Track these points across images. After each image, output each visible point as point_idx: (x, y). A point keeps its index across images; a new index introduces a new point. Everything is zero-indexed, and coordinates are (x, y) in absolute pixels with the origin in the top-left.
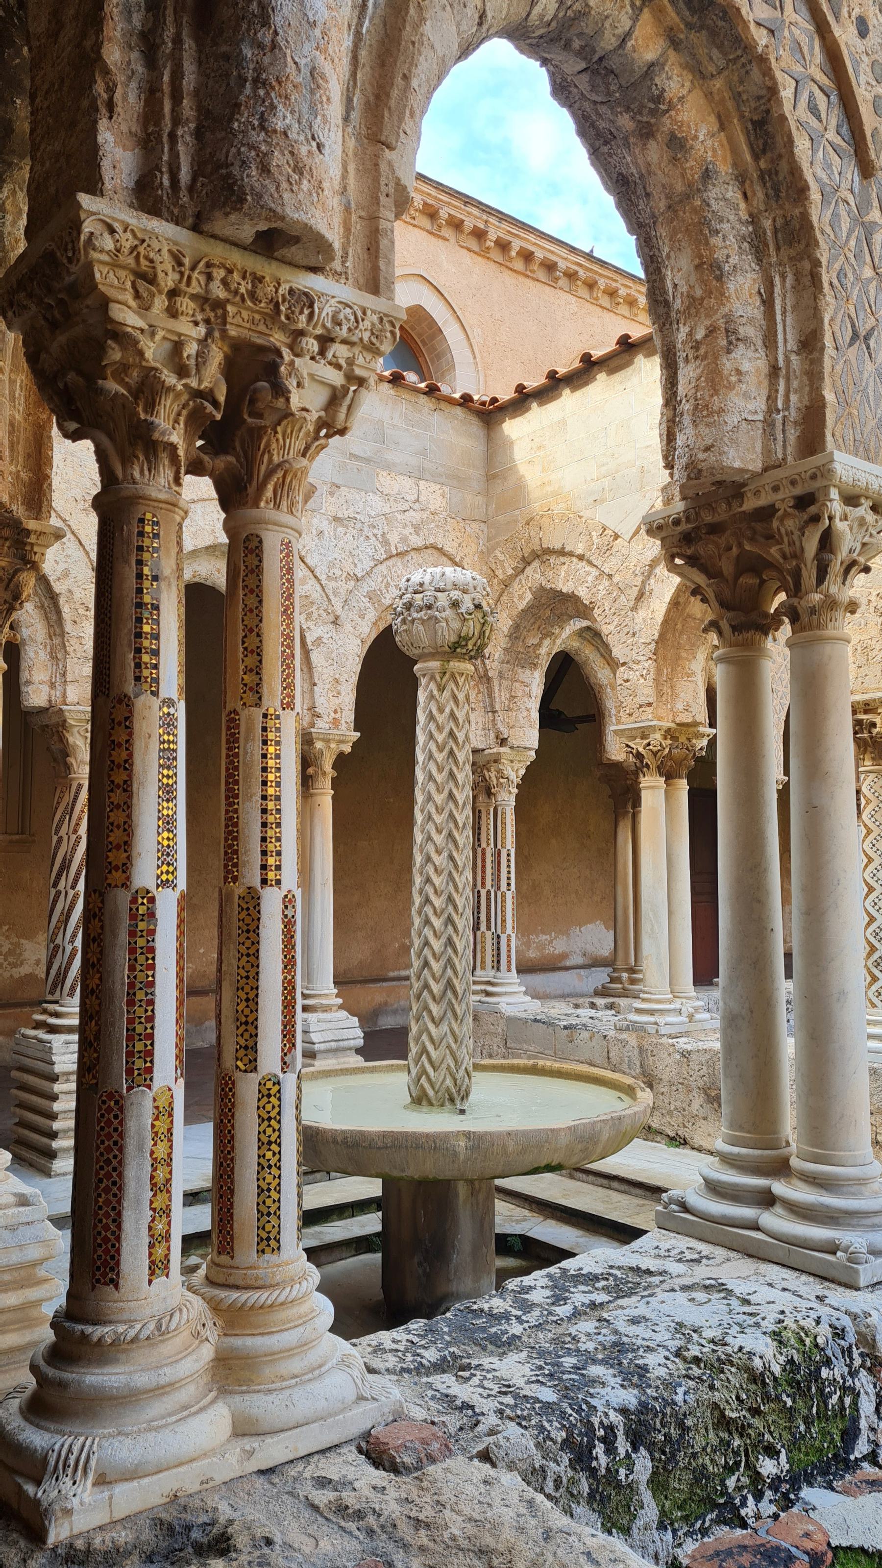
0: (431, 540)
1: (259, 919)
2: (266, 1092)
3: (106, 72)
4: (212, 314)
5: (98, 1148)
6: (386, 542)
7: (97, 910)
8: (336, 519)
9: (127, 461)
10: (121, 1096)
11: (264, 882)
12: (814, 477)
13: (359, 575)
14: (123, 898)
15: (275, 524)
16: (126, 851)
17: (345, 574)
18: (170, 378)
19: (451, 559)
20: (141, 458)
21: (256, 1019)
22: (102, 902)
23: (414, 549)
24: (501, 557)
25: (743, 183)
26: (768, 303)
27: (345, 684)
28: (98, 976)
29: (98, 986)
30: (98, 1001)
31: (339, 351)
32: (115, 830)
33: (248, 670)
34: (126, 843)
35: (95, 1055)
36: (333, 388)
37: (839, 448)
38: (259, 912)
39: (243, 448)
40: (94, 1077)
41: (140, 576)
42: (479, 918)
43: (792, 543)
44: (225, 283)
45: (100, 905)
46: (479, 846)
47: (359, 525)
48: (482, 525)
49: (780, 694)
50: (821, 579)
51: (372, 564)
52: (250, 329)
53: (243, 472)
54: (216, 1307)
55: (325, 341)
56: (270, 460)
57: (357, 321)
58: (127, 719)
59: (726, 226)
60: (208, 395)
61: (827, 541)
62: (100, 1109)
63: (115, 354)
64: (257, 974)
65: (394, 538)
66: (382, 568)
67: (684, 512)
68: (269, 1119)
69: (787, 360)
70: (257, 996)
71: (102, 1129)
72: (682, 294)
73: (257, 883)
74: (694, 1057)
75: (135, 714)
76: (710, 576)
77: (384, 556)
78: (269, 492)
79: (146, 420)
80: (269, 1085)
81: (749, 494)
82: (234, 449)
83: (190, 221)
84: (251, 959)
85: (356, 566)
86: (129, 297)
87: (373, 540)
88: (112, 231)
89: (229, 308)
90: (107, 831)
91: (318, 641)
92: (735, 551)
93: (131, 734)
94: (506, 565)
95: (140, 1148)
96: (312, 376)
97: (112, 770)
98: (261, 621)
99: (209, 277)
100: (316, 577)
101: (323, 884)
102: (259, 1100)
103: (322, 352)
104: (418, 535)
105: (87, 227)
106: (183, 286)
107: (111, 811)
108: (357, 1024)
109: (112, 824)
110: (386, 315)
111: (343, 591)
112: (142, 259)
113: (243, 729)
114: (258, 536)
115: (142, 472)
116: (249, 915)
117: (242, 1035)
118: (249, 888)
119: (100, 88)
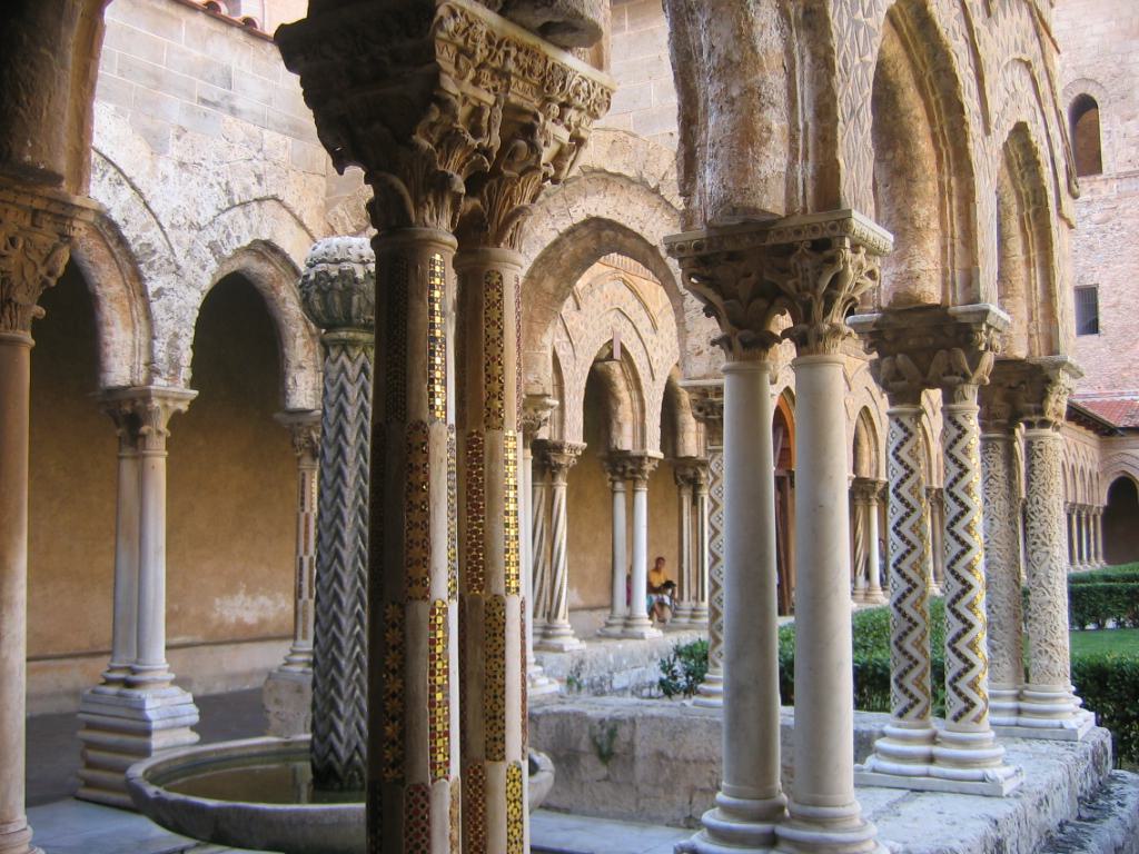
0: (273, 192)
1: (504, 624)
2: (512, 778)
4: (499, 84)
5: (407, 834)
6: (228, 192)
7: (397, 621)
8: (182, 164)
9: (419, 205)
10: (427, 788)
12: (833, 228)
13: (202, 225)
15: (513, 263)
16: (425, 567)
17: (188, 223)
19: (291, 212)
20: (432, 204)
21: (504, 714)
22: (403, 613)
23: (256, 200)
24: (342, 214)
26: (791, 76)
27: (184, 339)
28: (400, 681)
29: (400, 690)
30: (401, 704)
31: (572, 114)
32: (414, 546)
34: (425, 559)
35: (400, 752)
36: (562, 146)
37: (855, 209)
38: (504, 617)
39: (488, 192)
40: (399, 772)
42: (300, 586)
43: (805, 279)
44: (516, 59)
45: (401, 616)
46: (303, 510)
47: (203, 171)
48: (321, 178)
49: (582, 362)
50: (827, 312)
51: (216, 213)
52: (522, 97)
53: (486, 214)
55: (564, 106)
56: (511, 205)
57: (589, 93)
58: (424, 444)
60: (487, 152)
61: (837, 282)
62: (407, 800)
64: (504, 673)
65: (237, 188)
66: (224, 218)
67: (707, 239)
68: (515, 801)
70: (504, 693)
71: (411, 817)
72: (719, 56)
74: (542, 721)
75: (431, 440)
76: (724, 298)
77: (227, 205)
79: (443, 172)
80: (514, 771)
81: (772, 232)
82: (482, 193)
83: (499, 8)
84: (499, 660)
85: (199, 214)
87: (217, 188)
88: (454, 15)
89: (513, 79)
90: (405, 548)
91: (159, 293)
92: (753, 278)
93: (427, 459)
94: (347, 222)
95: (443, 833)
97: (410, 491)
98: (502, 351)
100: (159, 224)
101: (157, 553)
102: (507, 785)
104: (260, 184)
106: (489, 61)
107: (410, 529)
108: (793, 713)
109: (411, 541)
110: (606, 88)
111: (185, 240)
112: (470, 41)
113: (487, 447)
114: (498, 273)
115: (431, 217)
116: (495, 620)
117: (491, 729)
118: (496, 596)
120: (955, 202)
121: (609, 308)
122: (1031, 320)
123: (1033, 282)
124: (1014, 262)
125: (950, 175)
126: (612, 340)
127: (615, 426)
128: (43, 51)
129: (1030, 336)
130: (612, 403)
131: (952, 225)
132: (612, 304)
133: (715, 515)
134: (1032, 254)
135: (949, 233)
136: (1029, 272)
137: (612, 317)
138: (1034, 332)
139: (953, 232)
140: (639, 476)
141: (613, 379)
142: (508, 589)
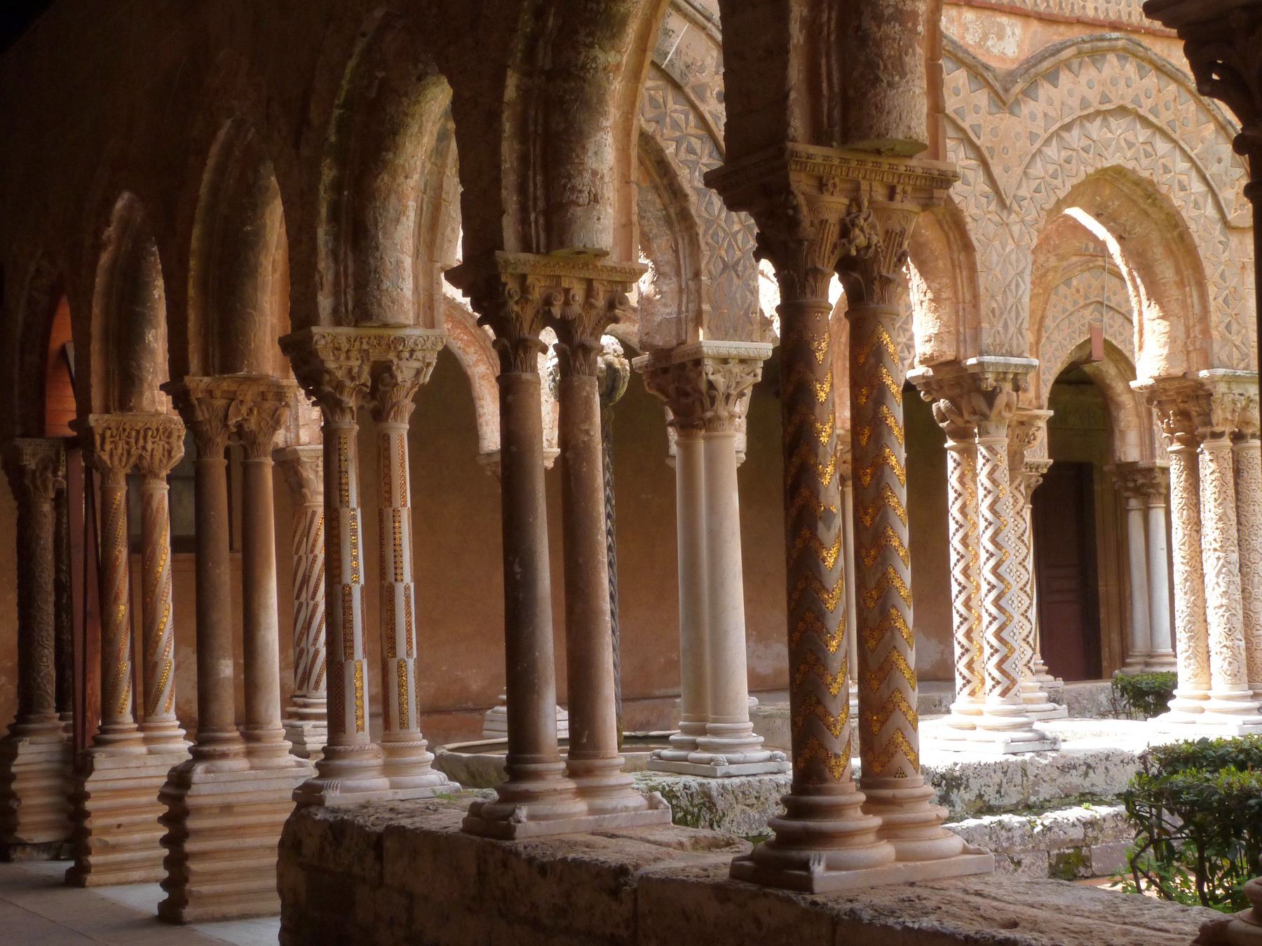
3: (319, 272)
9: (333, 414)
11: (396, 580)
14: (339, 588)
18: (348, 383)
25: (657, 190)
31: (419, 354)
33: (386, 492)
41: (340, 460)
44: (368, 343)
54: (384, 748)
55: (412, 352)
59: (649, 215)
60: (364, 385)
63: (327, 378)
69: (687, 285)
73: (393, 581)
78: (392, 414)
86: (332, 358)
88: (324, 337)
96: (407, 367)
99: (362, 343)
103: (411, 356)
105: (315, 339)
119: (317, 278)
120: (965, 273)
121: (1082, 303)
122: (1188, 337)
123: (1189, 301)
124: (1164, 284)
125: (959, 252)
126: (1089, 341)
127: (1117, 434)
128: (249, 310)
129: (1188, 352)
130: (1112, 408)
131: (963, 293)
132: (1086, 297)
133: (1021, 531)
134: (1185, 273)
135: (961, 300)
136: (1184, 295)
137: (1088, 315)
138: (1191, 348)
139: (964, 298)
140: (1152, 491)
141: (1108, 381)
142: (396, 580)
